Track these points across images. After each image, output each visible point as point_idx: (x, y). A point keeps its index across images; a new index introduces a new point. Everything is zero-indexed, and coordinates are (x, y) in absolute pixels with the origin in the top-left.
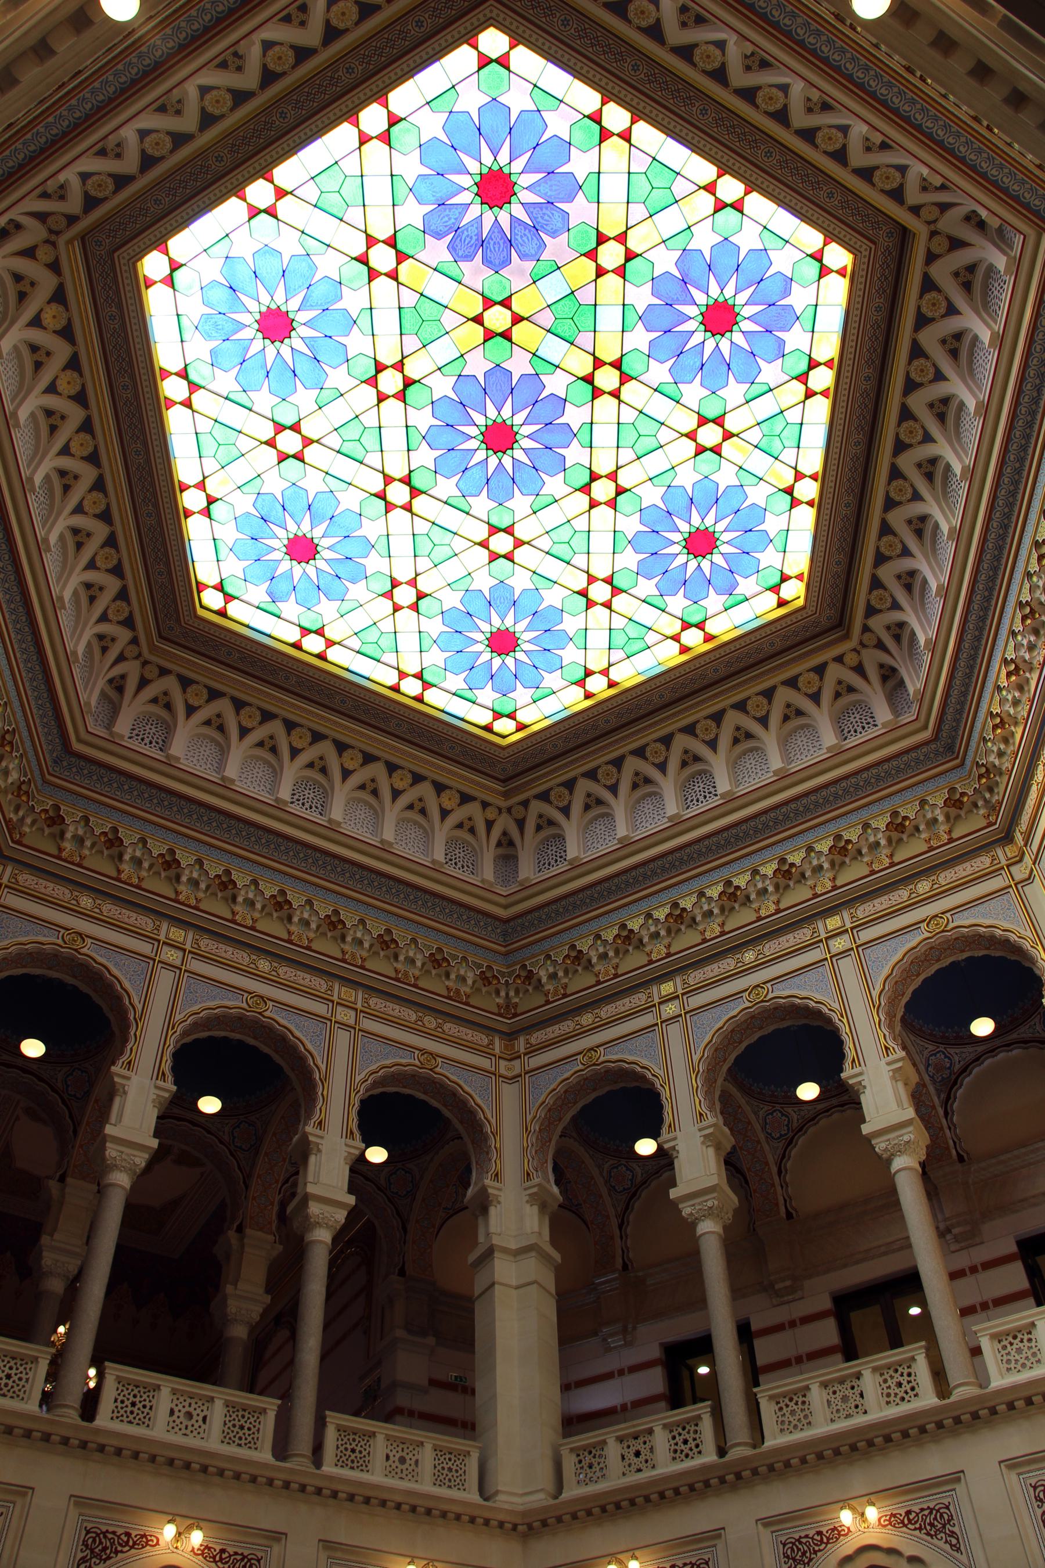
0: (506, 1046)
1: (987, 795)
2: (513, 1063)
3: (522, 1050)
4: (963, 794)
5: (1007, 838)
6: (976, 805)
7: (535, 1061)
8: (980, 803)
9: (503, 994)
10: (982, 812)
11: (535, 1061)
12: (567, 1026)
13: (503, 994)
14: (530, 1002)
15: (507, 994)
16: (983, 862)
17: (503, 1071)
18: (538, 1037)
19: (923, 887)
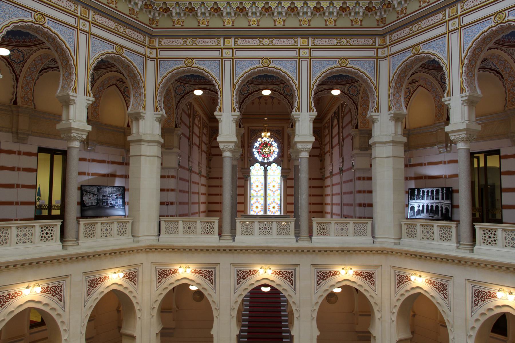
0: (150, 40)
1: (383, 13)
2: (153, 50)
3: (157, 46)
4: (373, 7)
5: (383, 36)
6: (376, 13)
7: (163, 54)
8: (378, 14)
9: (152, 14)
10: (377, 18)
11: (163, 54)
12: (179, 42)
13: (152, 14)
14: (164, 23)
15: (154, 14)
16: (368, 41)
17: (149, 55)
18: (165, 42)
19: (344, 42)
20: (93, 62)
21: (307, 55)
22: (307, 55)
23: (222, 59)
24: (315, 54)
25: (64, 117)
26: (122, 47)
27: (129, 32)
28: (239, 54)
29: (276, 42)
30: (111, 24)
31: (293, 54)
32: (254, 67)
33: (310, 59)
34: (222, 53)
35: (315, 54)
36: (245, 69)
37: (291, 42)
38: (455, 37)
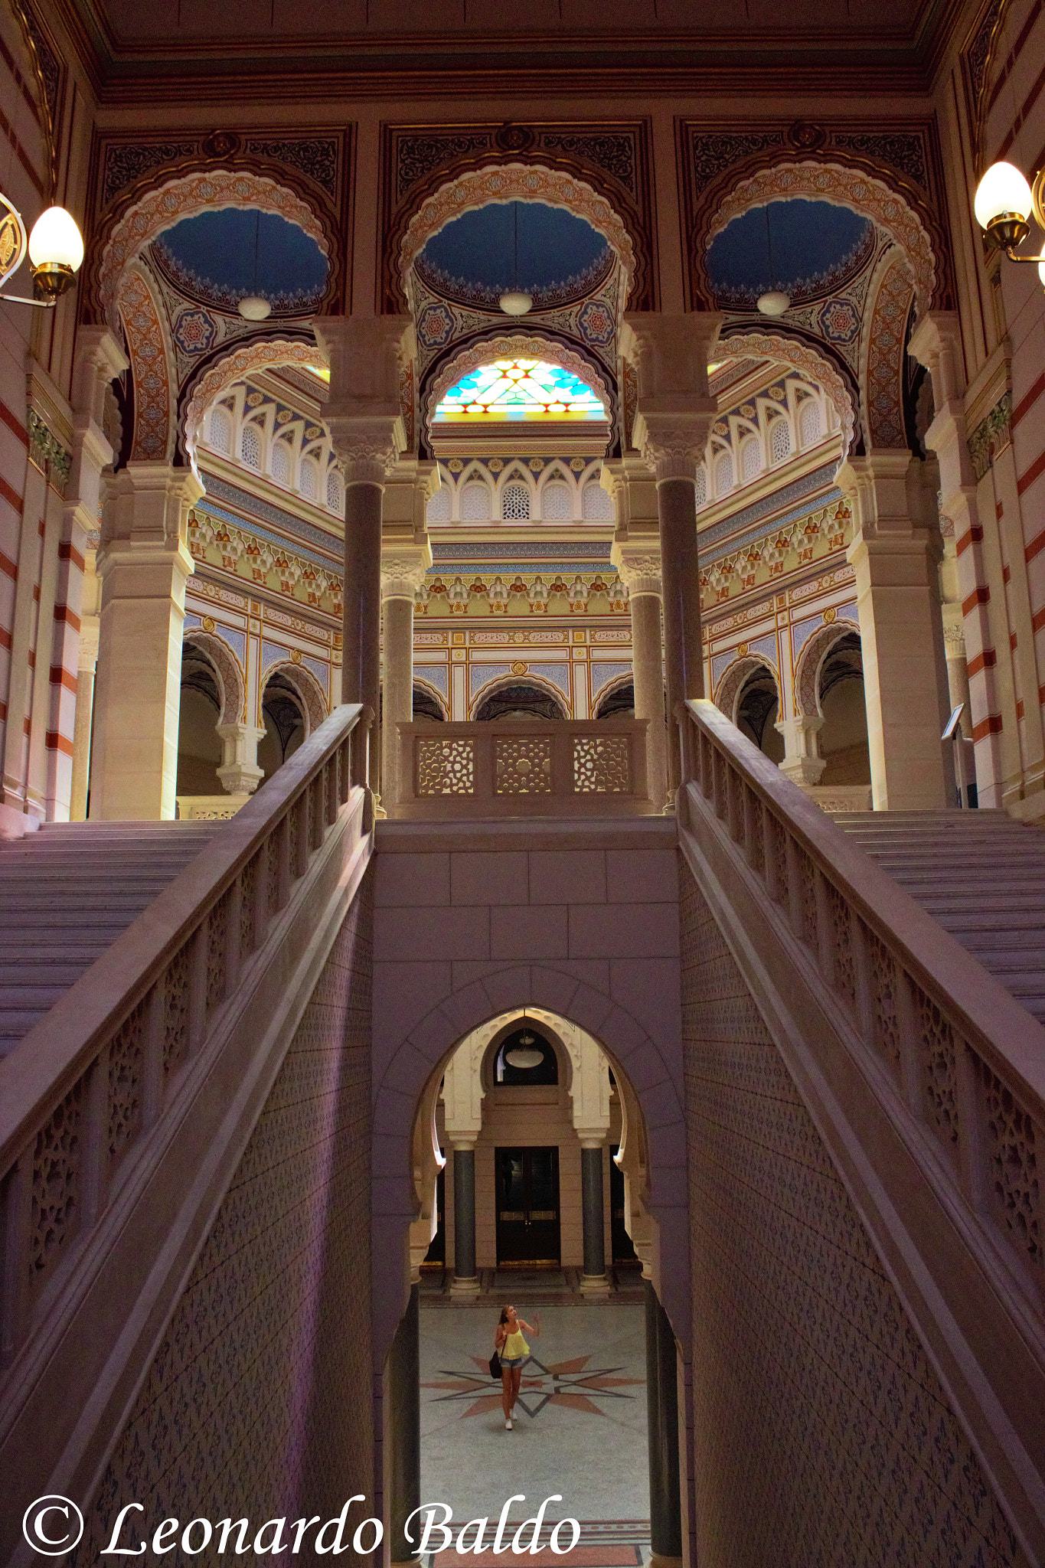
20: (265, 677)
21: (585, 657)
22: (585, 657)
23: (450, 664)
24: (597, 654)
25: (228, 758)
26: (300, 651)
27: (310, 629)
28: (477, 656)
29: (535, 637)
30: (287, 620)
31: (562, 655)
32: (501, 675)
33: (589, 662)
34: (450, 656)
35: (597, 654)
36: (487, 681)
37: (559, 636)
38: (785, 635)
